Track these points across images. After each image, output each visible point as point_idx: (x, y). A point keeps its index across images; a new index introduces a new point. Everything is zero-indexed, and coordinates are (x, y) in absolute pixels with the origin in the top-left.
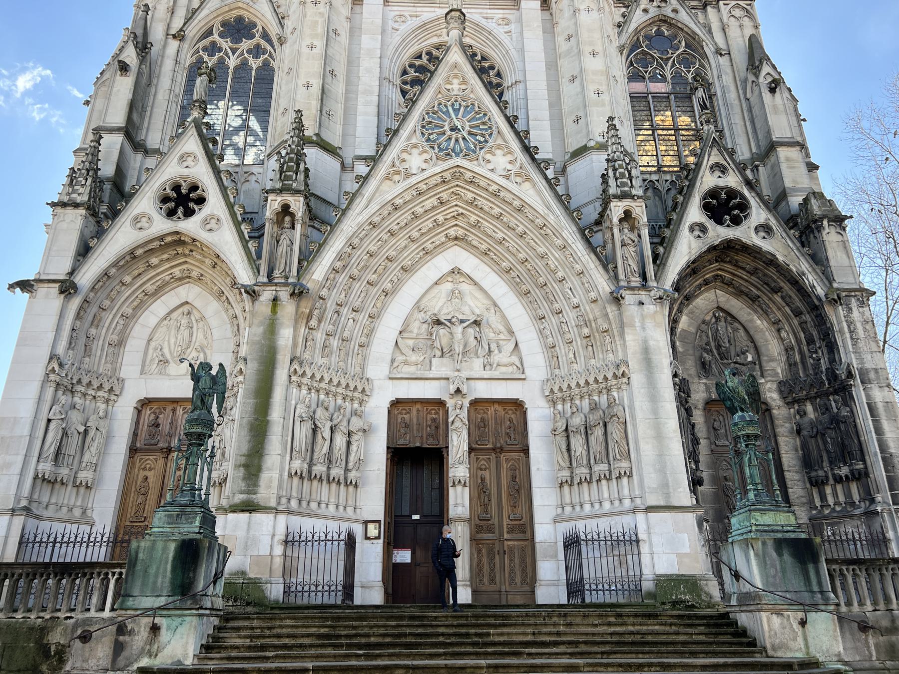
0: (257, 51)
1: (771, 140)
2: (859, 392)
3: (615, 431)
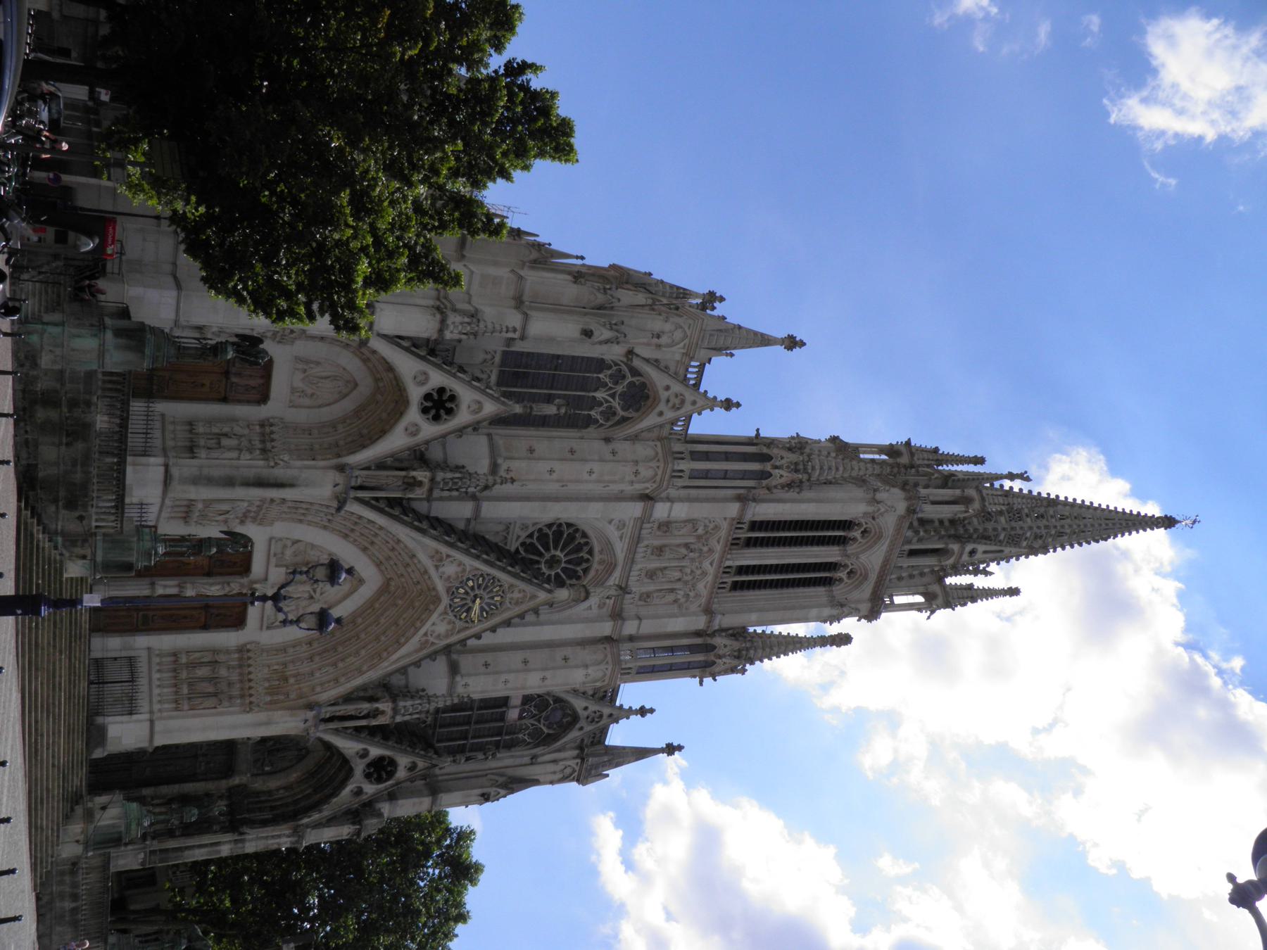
0: (609, 413)
1: (442, 792)
2: (229, 837)
3: (211, 702)
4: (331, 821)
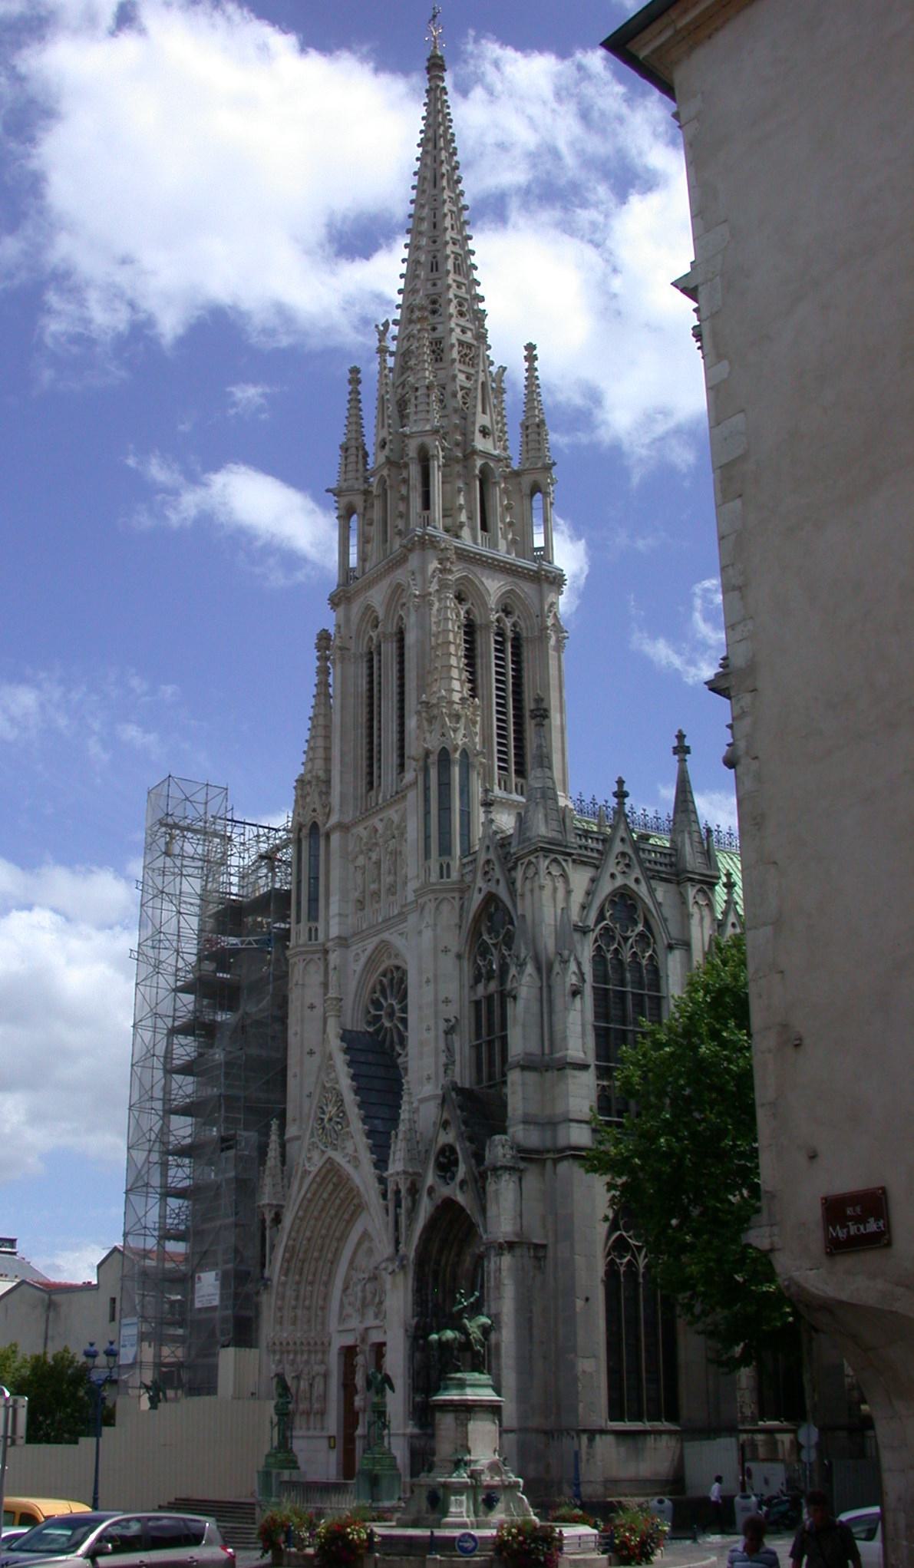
4: (483, 1210)
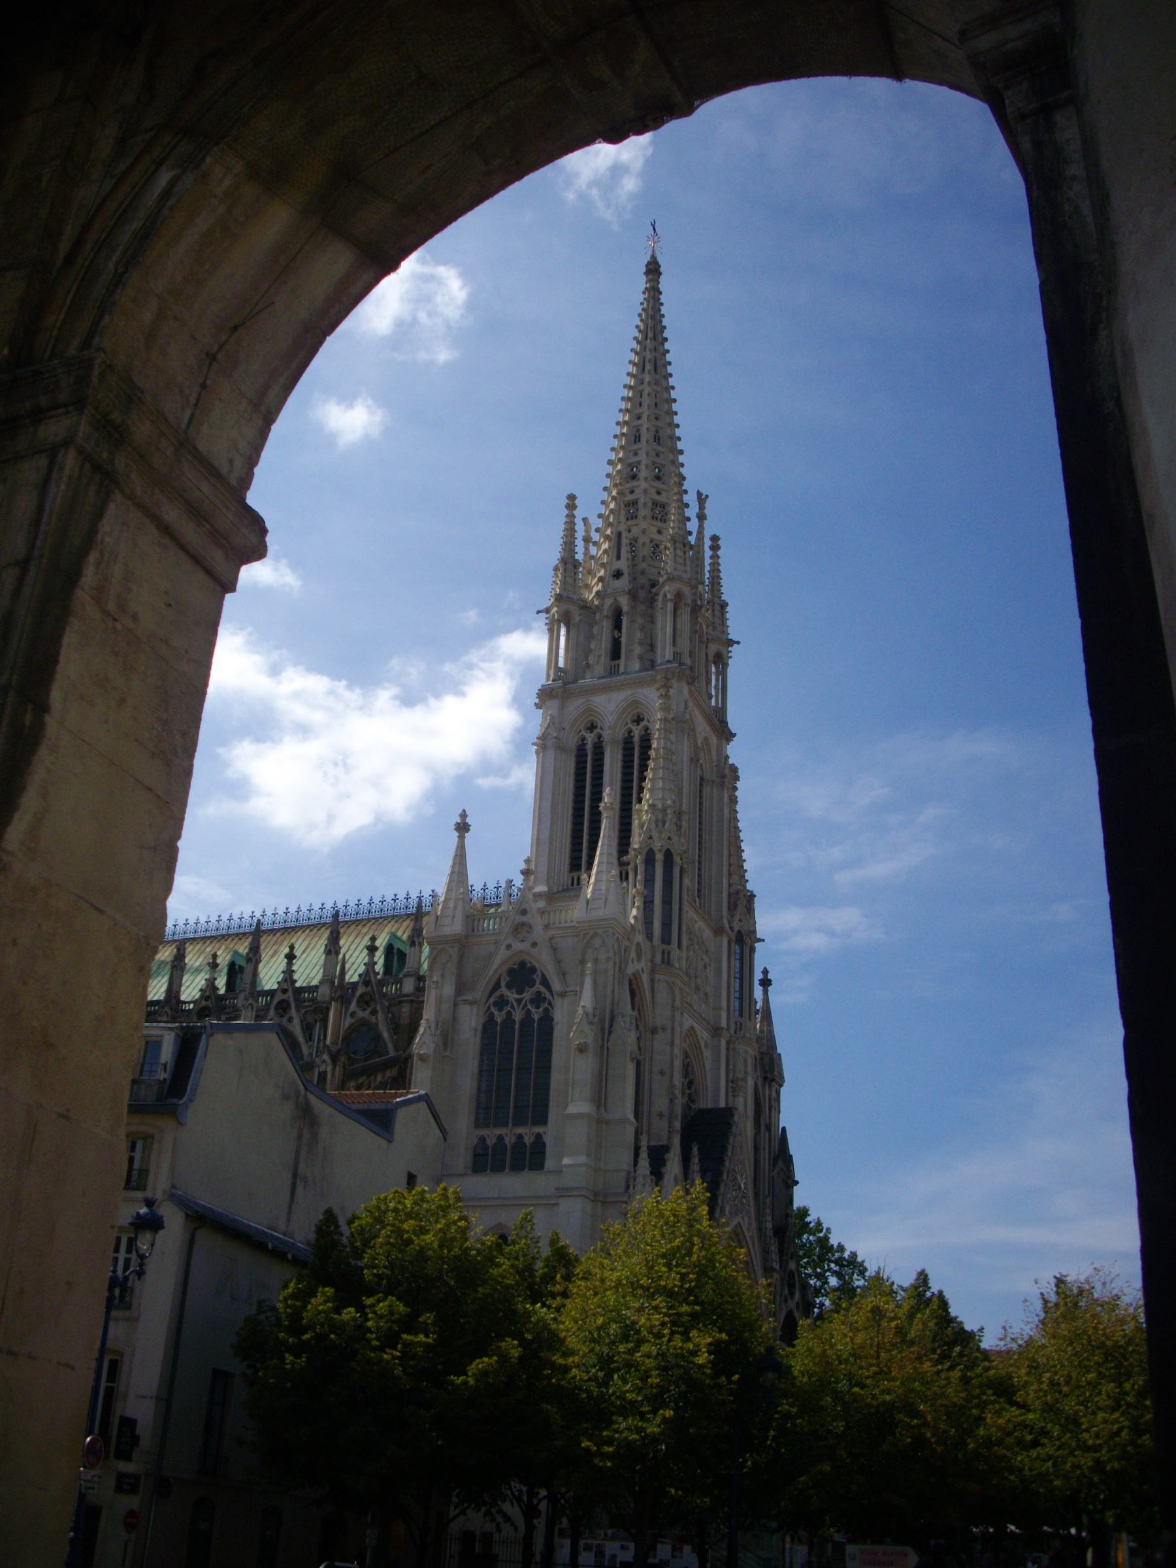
0: (538, 1000)
